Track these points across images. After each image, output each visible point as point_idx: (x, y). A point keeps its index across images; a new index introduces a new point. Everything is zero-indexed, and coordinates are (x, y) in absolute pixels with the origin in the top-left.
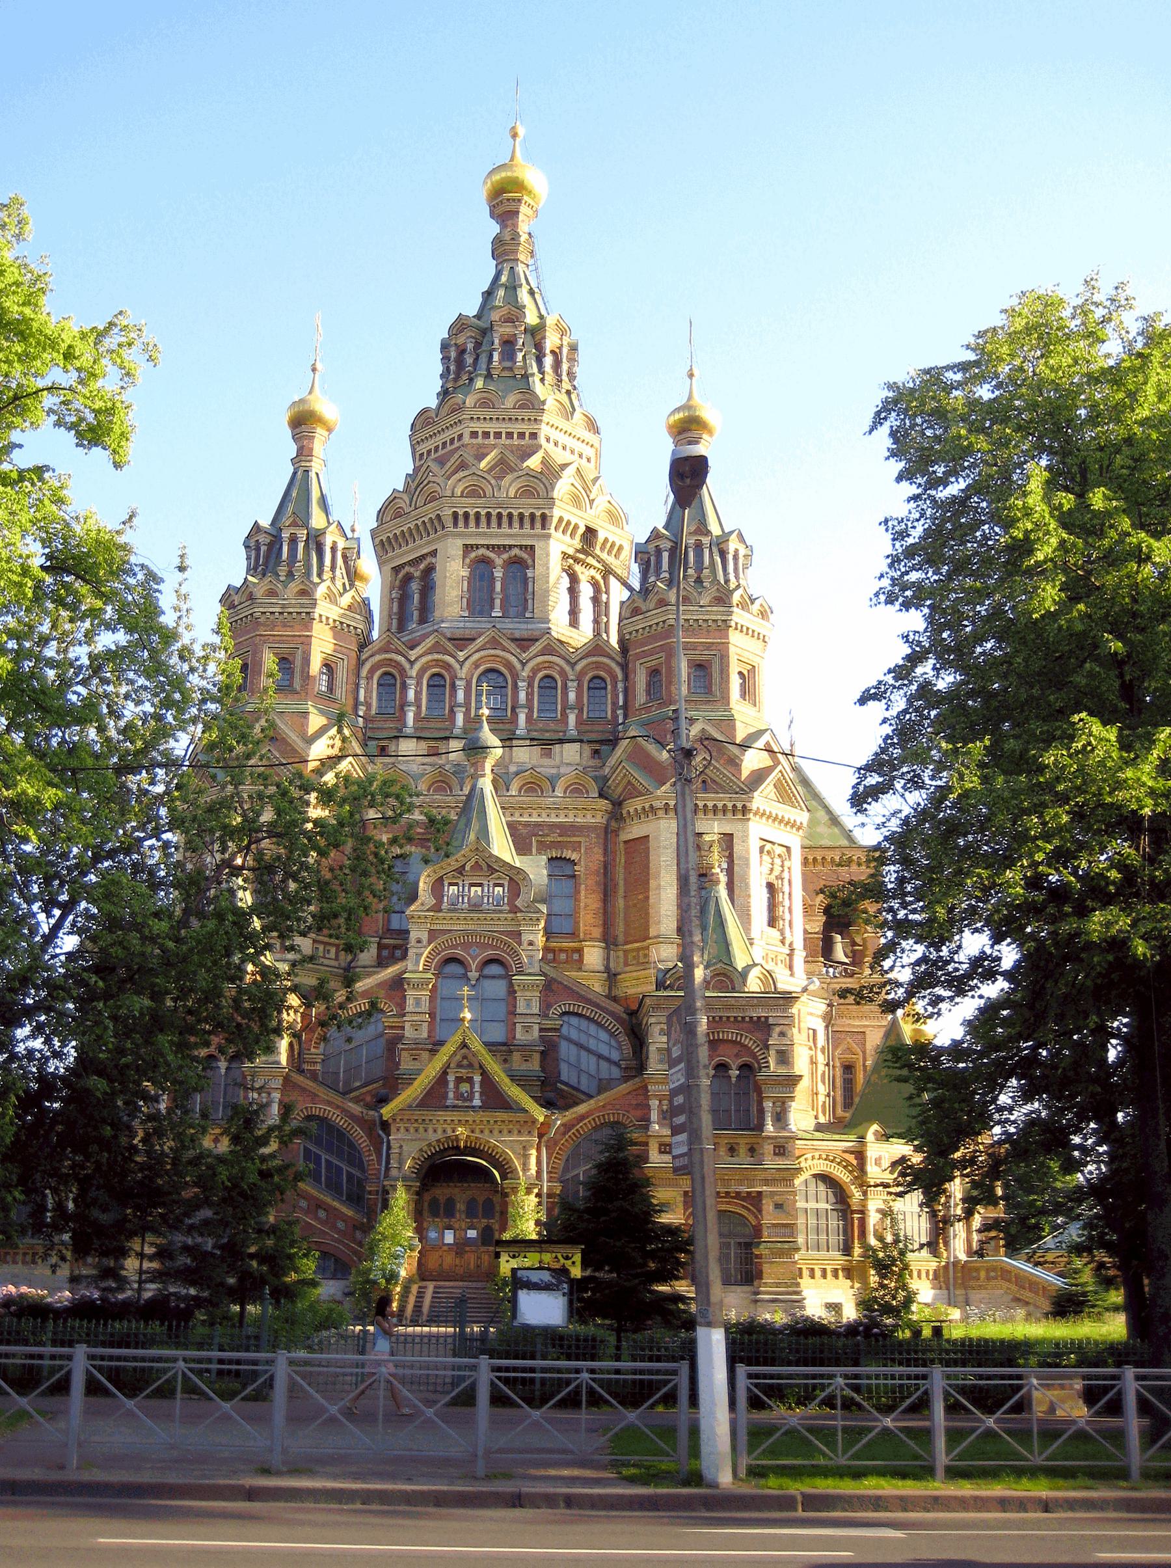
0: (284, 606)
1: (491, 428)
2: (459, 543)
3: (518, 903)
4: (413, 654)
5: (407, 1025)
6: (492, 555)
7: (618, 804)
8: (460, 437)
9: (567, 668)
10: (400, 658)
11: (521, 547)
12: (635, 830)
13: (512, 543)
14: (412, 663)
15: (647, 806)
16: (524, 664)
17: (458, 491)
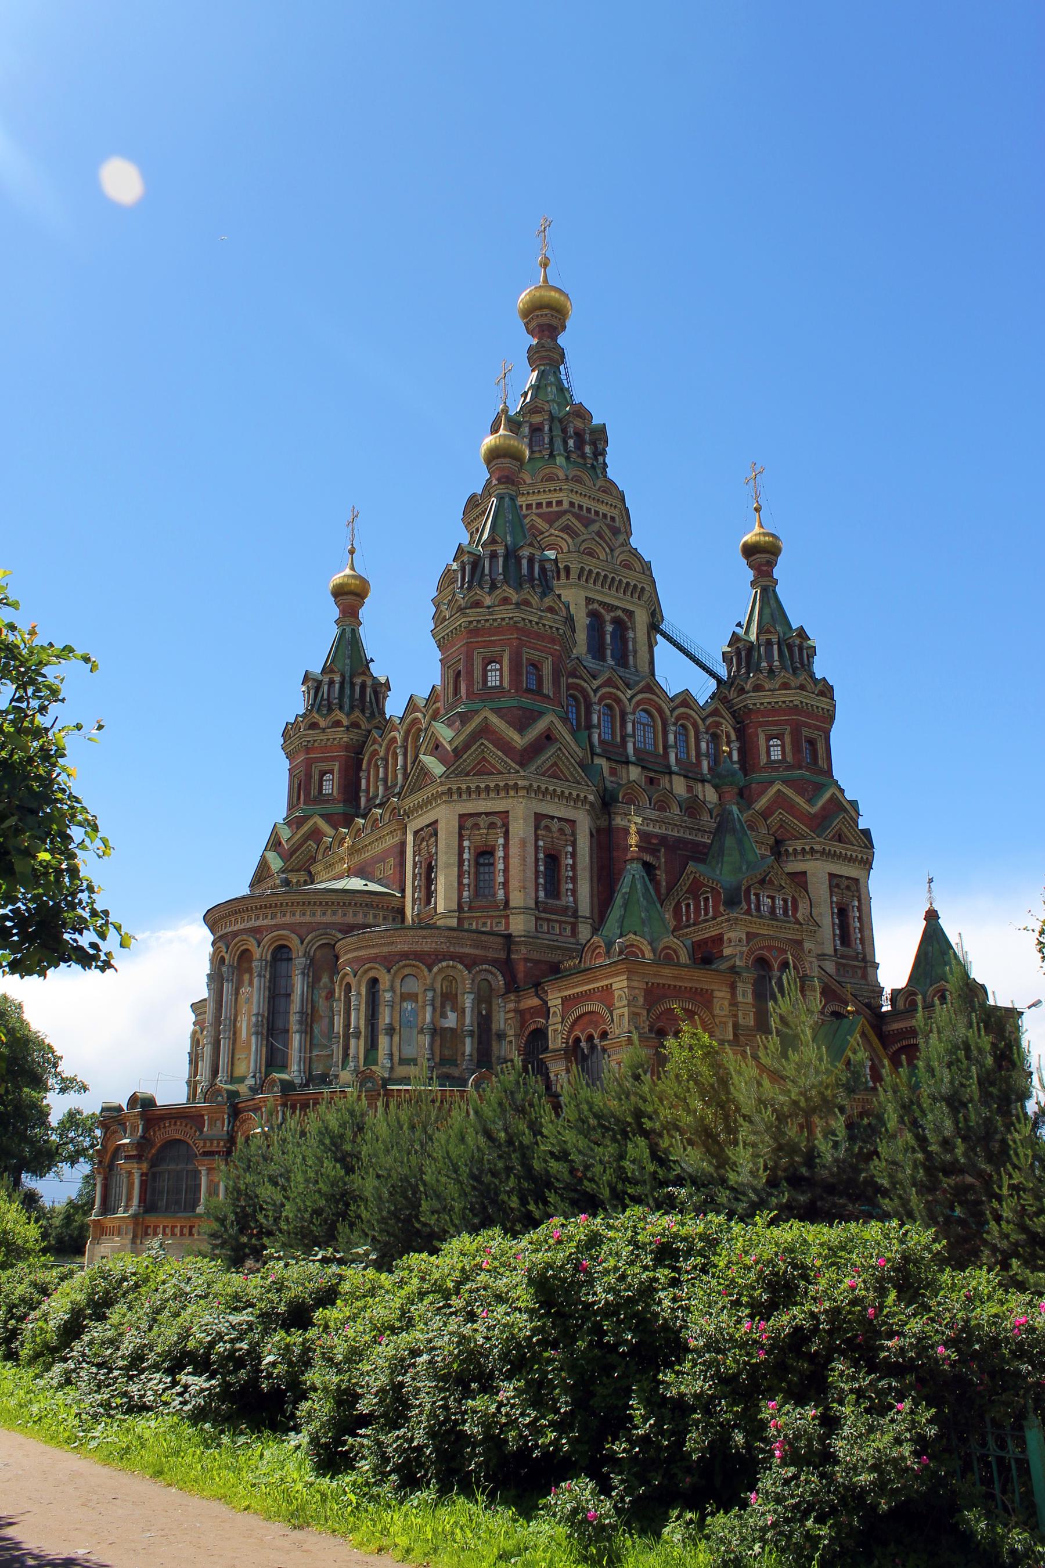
0: (541, 617)
1: (586, 503)
2: (583, 594)
3: (799, 915)
4: (596, 683)
5: (740, 1013)
6: (603, 611)
7: (778, 843)
8: (559, 503)
9: (700, 722)
10: (586, 685)
11: (624, 610)
12: (793, 866)
13: (619, 605)
14: (595, 691)
15: (807, 848)
16: (672, 712)
17: (582, 549)
